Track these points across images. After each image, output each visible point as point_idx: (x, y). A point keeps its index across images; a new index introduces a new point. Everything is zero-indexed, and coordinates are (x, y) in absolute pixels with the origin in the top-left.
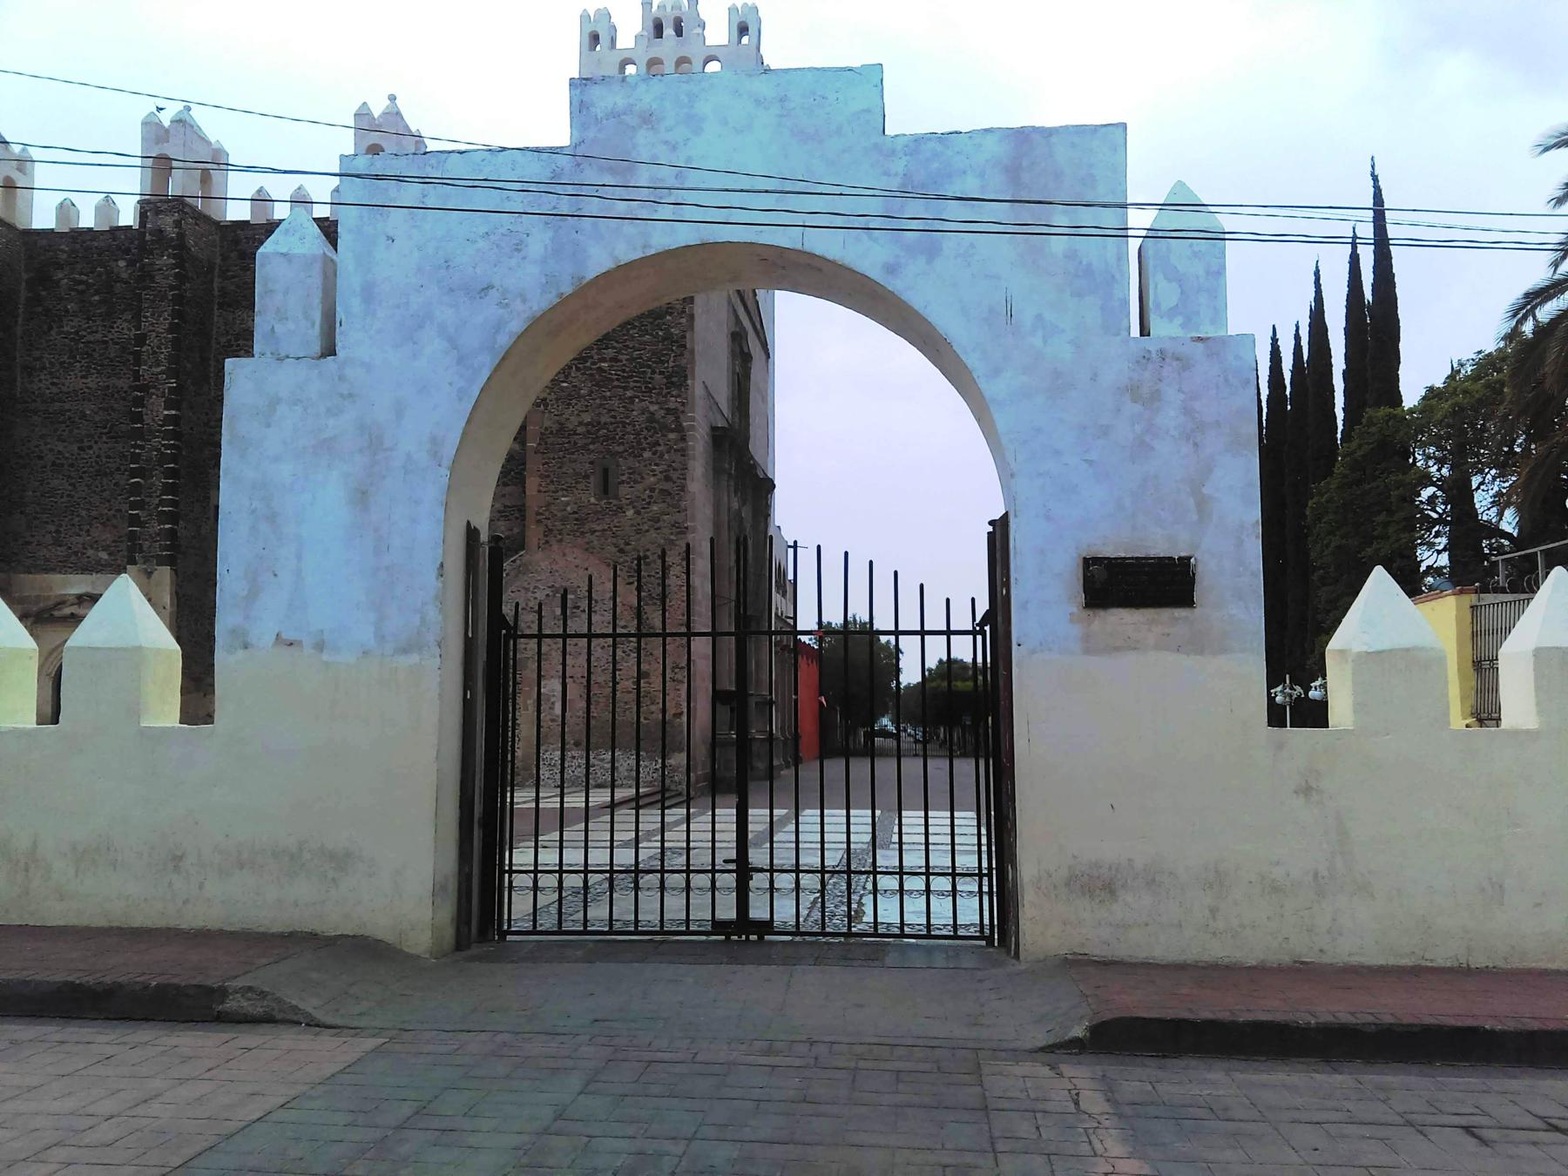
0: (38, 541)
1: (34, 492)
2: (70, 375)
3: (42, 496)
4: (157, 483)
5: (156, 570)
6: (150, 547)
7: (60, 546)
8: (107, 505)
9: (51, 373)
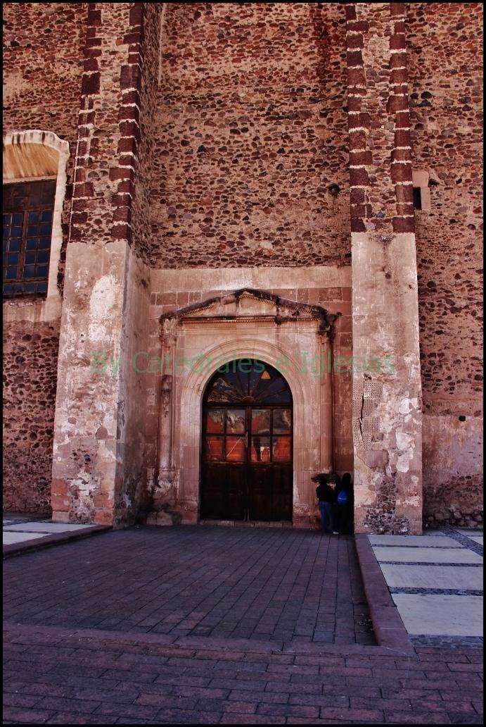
0: (183, 233)
1: (178, 179)
2: (219, 60)
3: (187, 183)
4: (387, 132)
5: (394, 237)
6: (383, 209)
7: (211, 236)
8: (269, 189)
9: (197, 60)
